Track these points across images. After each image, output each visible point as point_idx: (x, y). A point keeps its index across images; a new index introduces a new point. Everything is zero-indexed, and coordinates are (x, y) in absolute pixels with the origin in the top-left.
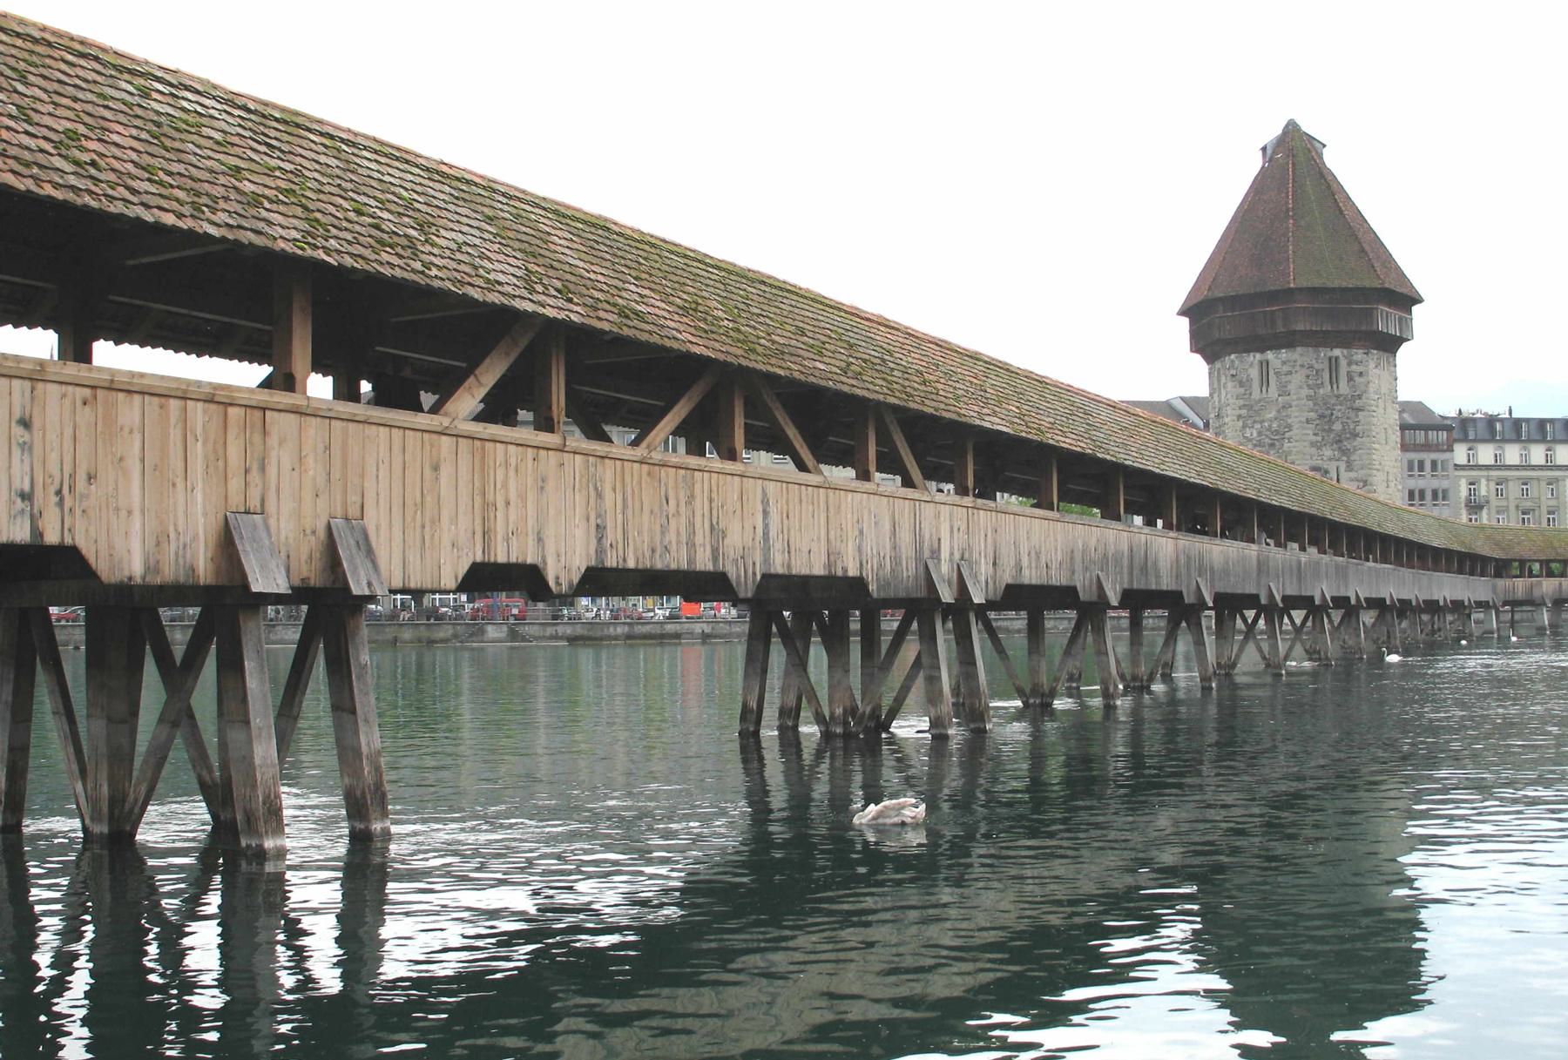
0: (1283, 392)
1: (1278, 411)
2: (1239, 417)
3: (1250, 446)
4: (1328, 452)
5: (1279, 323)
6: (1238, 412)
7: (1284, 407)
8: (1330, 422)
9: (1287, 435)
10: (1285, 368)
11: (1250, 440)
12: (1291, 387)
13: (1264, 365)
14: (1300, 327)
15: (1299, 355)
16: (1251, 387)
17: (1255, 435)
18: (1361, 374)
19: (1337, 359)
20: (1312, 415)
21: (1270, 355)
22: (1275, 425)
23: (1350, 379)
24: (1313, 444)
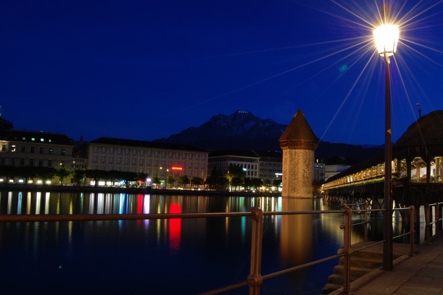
0: (298, 156)
1: (297, 160)
2: (290, 160)
4: (305, 167)
7: (298, 159)
8: (306, 162)
9: (299, 164)
11: (292, 164)
15: (302, 151)
16: (293, 155)
17: (293, 164)
20: (303, 161)
21: (296, 150)
22: (297, 162)
23: (309, 155)
24: (303, 166)
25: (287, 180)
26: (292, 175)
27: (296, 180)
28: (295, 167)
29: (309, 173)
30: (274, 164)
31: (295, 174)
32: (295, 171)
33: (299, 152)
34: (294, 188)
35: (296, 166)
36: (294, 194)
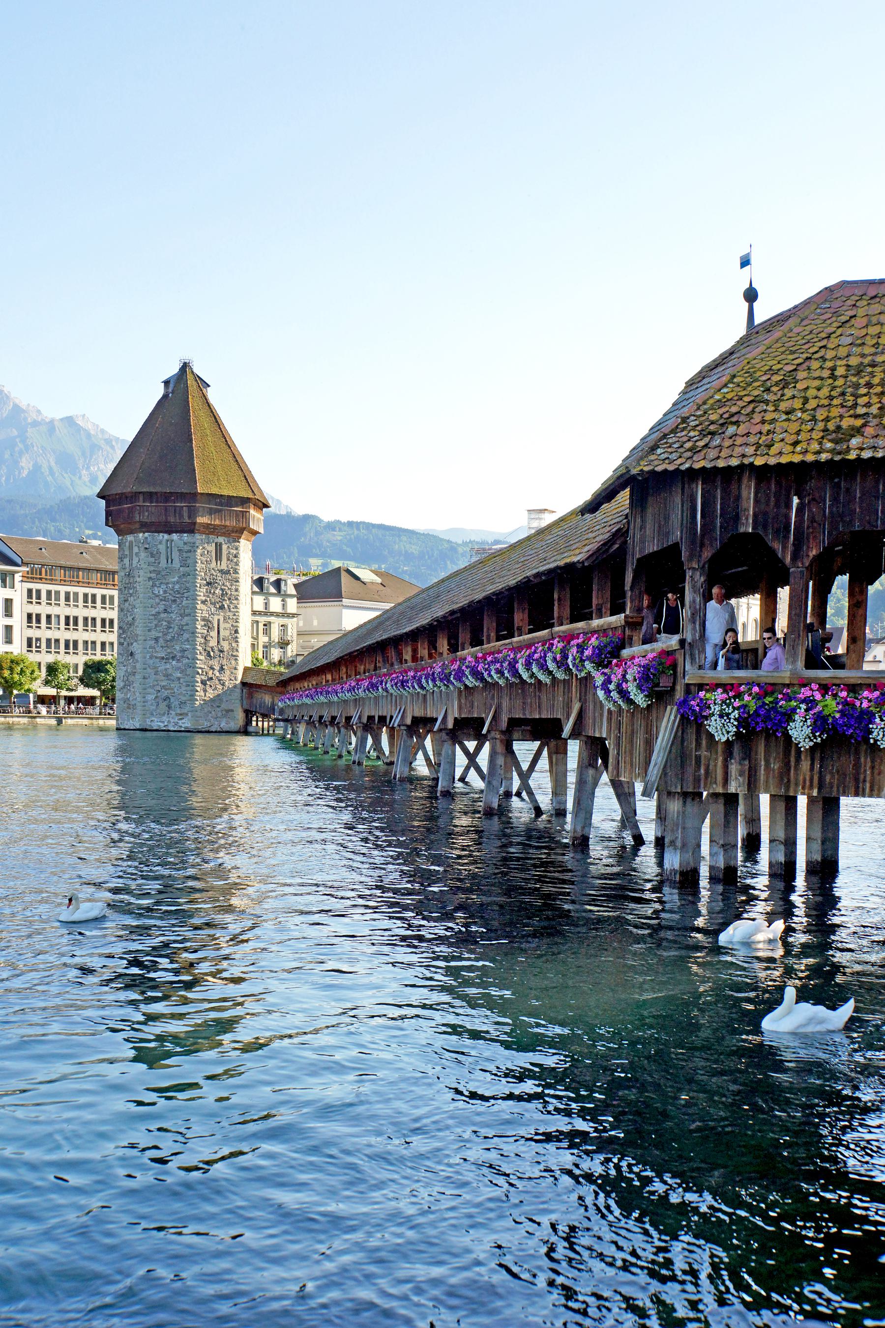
1: (179, 577)
2: (150, 578)
3: (157, 600)
5: (186, 515)
6: (149, 575)
9: (186, 595)
10: (186, 548)
11: (157, 596)
12: (188, 562)
13: (169, 544)
14: (200, 520)
17: (161, 592)
18: (236, 556)
19: (221, 544)
21: (175, 536)
23: (228, 560)
25: (137, 661)
26: (156, 639)
27: (174, 663)
28: (171, 607)
29: (227, 633)
30: (86, 596)
31: (169, 638)
32: (169, 622)
33: (185, 543)
34: (166, 693)
35: (175, 601)
36: (165, 718)
